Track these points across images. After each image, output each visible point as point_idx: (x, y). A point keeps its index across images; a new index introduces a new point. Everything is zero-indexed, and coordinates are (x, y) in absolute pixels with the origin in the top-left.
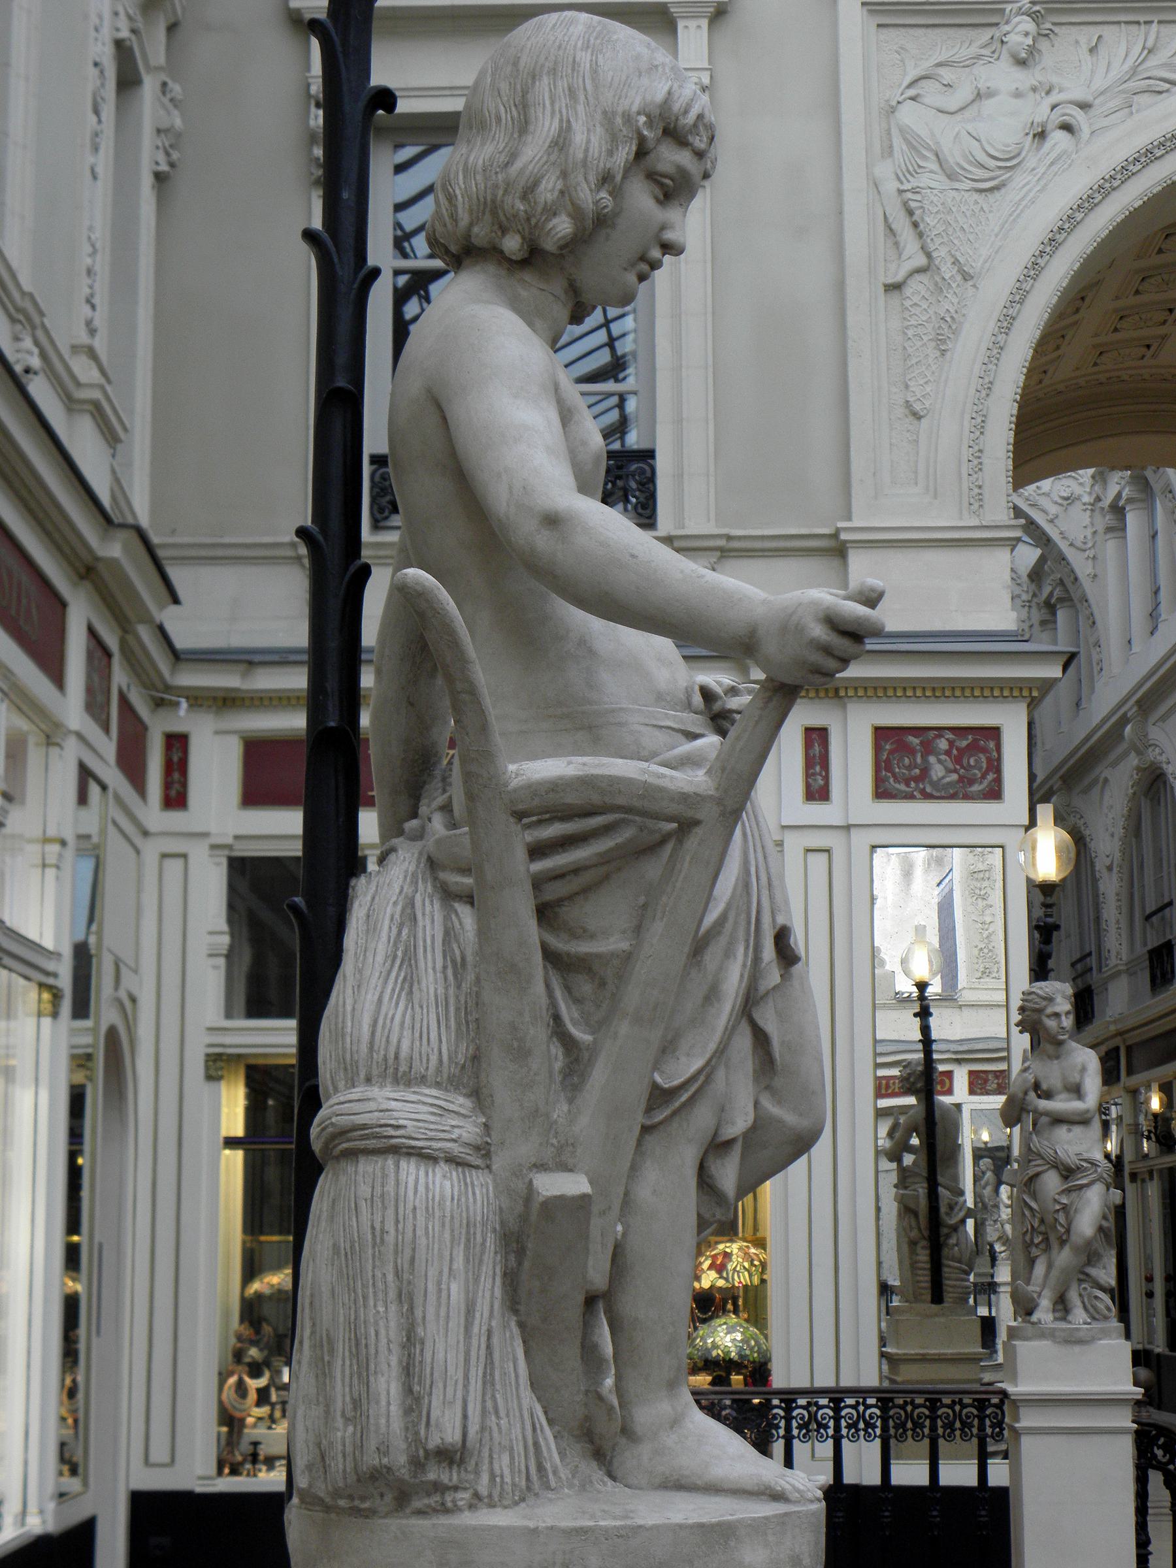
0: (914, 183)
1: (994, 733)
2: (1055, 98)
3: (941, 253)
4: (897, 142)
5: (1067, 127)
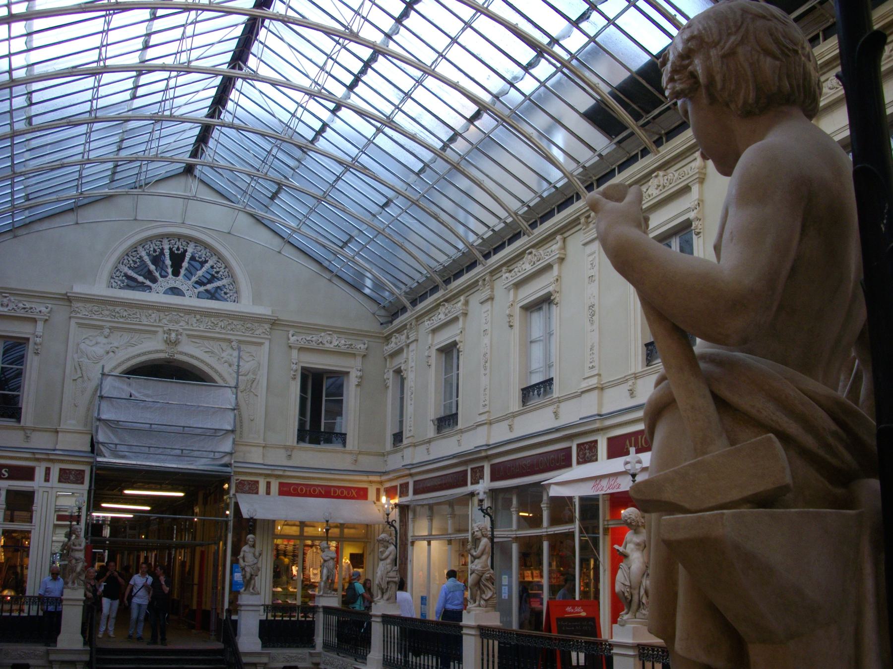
0: (81, 360)
1: (83, 471)
2: (111, 345)
3: (85, 375)
4: (79, 351)
5: (113, 352)
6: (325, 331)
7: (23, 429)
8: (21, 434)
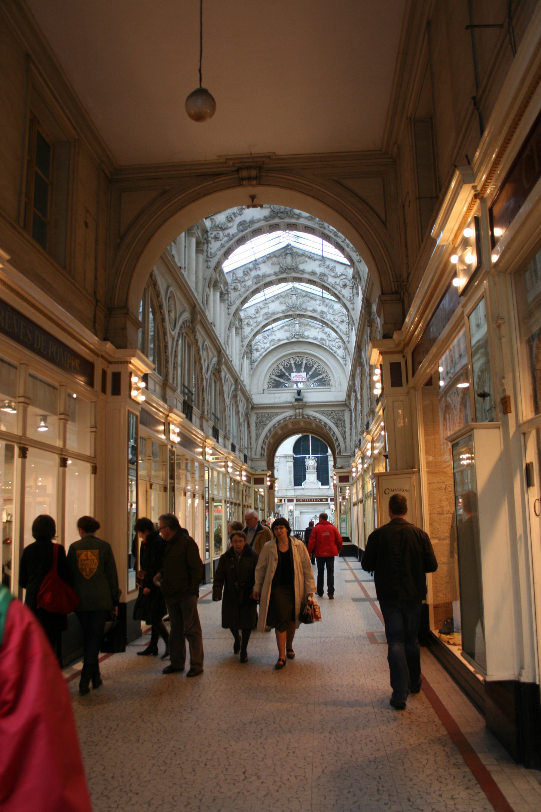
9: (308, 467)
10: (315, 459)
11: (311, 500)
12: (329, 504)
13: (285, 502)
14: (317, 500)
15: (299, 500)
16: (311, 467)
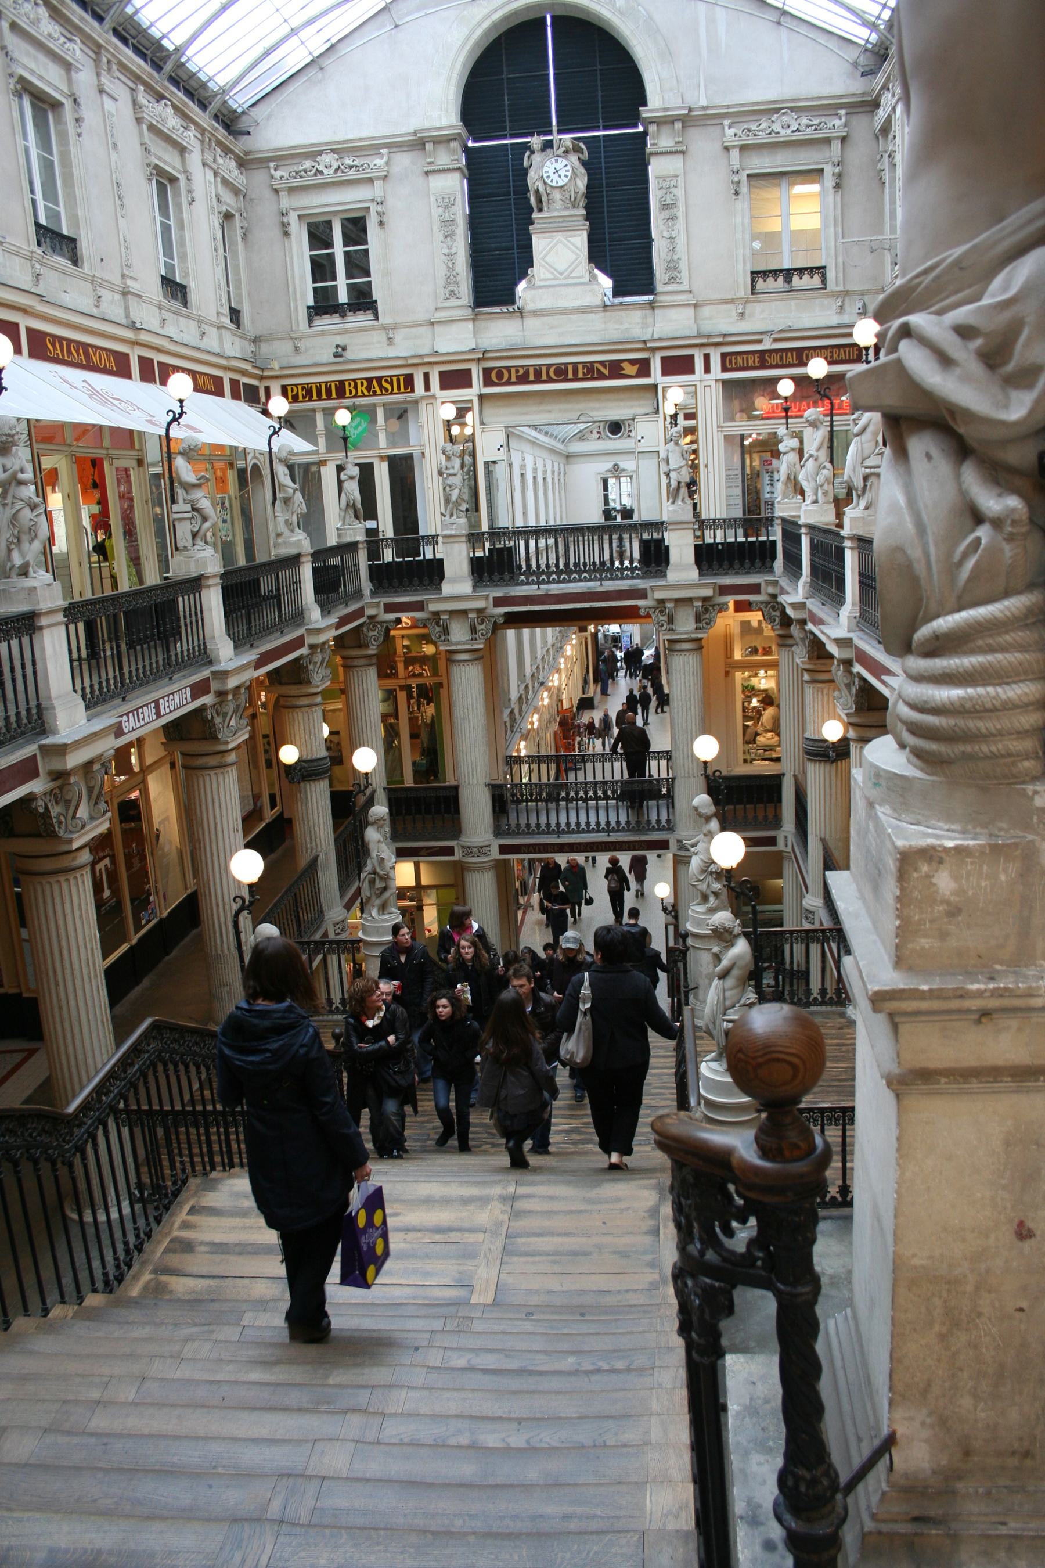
6: (777, 111)
7: (384, 328)
8: (379, 337)
9: (539, 201)
10: (577, 150)
11: (561, 373)
12: (655, 386)
13: (427, 388)
14: (592, 372)
15: (500, 375)
16: (557, 195)
